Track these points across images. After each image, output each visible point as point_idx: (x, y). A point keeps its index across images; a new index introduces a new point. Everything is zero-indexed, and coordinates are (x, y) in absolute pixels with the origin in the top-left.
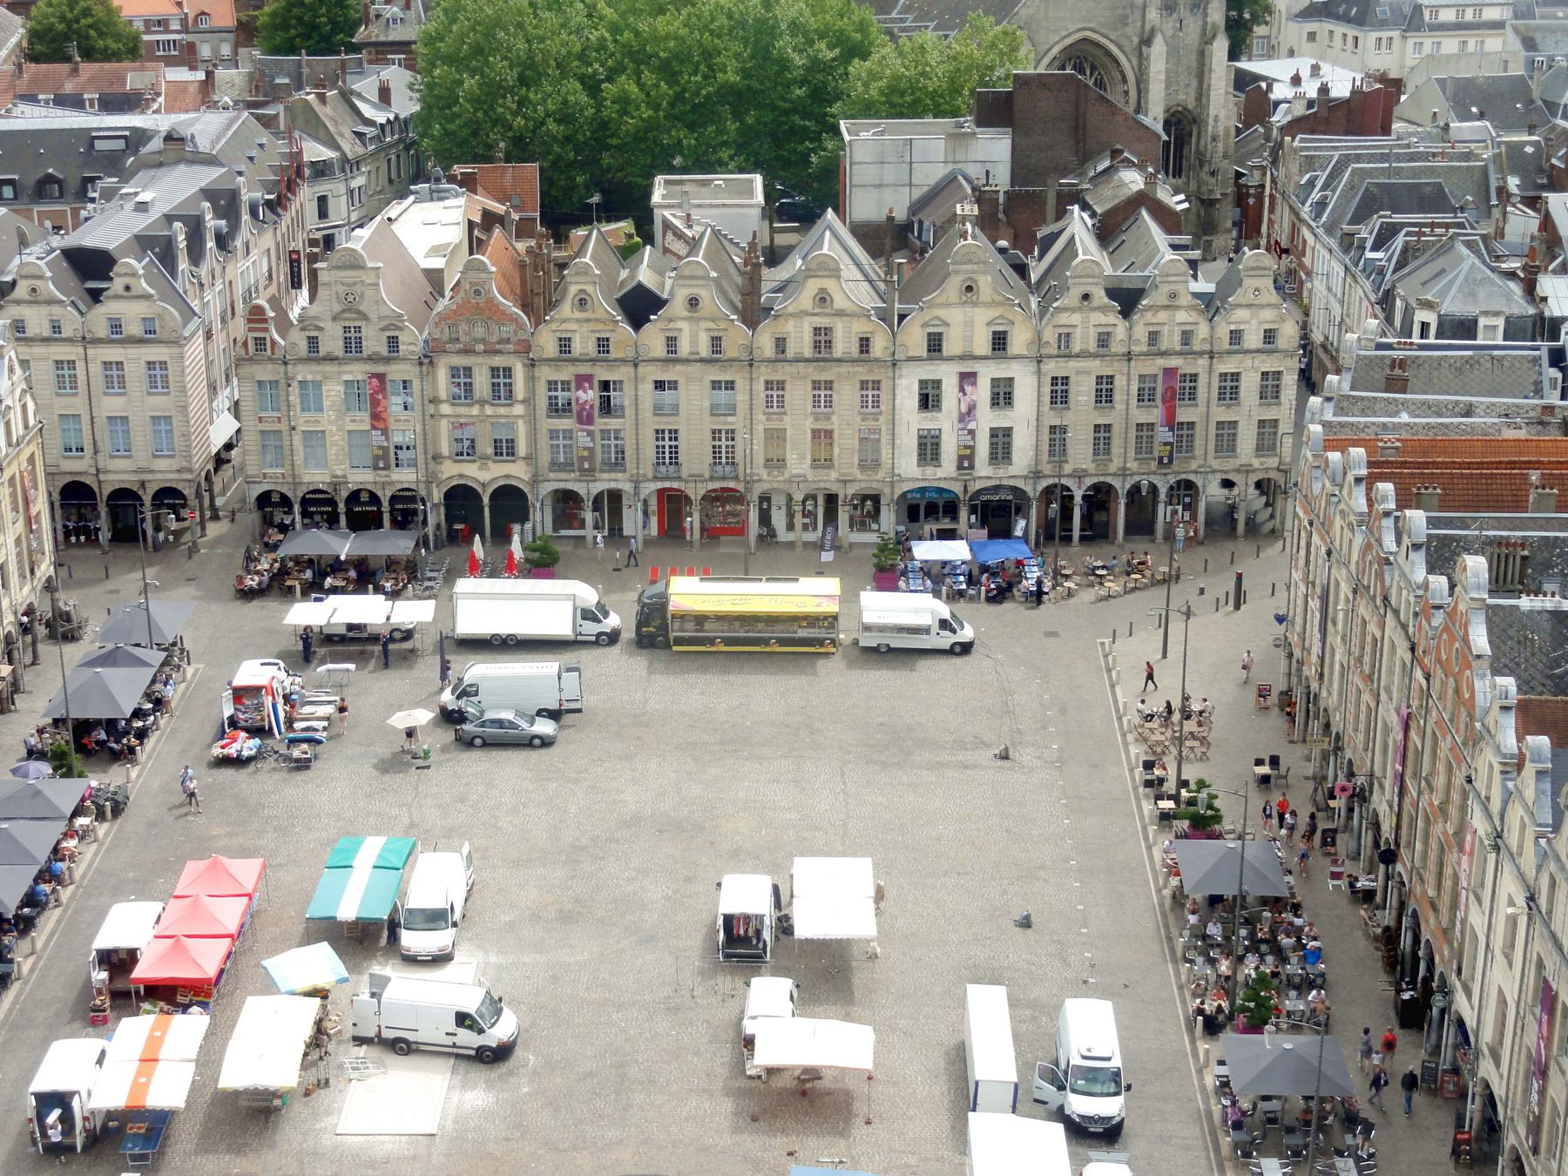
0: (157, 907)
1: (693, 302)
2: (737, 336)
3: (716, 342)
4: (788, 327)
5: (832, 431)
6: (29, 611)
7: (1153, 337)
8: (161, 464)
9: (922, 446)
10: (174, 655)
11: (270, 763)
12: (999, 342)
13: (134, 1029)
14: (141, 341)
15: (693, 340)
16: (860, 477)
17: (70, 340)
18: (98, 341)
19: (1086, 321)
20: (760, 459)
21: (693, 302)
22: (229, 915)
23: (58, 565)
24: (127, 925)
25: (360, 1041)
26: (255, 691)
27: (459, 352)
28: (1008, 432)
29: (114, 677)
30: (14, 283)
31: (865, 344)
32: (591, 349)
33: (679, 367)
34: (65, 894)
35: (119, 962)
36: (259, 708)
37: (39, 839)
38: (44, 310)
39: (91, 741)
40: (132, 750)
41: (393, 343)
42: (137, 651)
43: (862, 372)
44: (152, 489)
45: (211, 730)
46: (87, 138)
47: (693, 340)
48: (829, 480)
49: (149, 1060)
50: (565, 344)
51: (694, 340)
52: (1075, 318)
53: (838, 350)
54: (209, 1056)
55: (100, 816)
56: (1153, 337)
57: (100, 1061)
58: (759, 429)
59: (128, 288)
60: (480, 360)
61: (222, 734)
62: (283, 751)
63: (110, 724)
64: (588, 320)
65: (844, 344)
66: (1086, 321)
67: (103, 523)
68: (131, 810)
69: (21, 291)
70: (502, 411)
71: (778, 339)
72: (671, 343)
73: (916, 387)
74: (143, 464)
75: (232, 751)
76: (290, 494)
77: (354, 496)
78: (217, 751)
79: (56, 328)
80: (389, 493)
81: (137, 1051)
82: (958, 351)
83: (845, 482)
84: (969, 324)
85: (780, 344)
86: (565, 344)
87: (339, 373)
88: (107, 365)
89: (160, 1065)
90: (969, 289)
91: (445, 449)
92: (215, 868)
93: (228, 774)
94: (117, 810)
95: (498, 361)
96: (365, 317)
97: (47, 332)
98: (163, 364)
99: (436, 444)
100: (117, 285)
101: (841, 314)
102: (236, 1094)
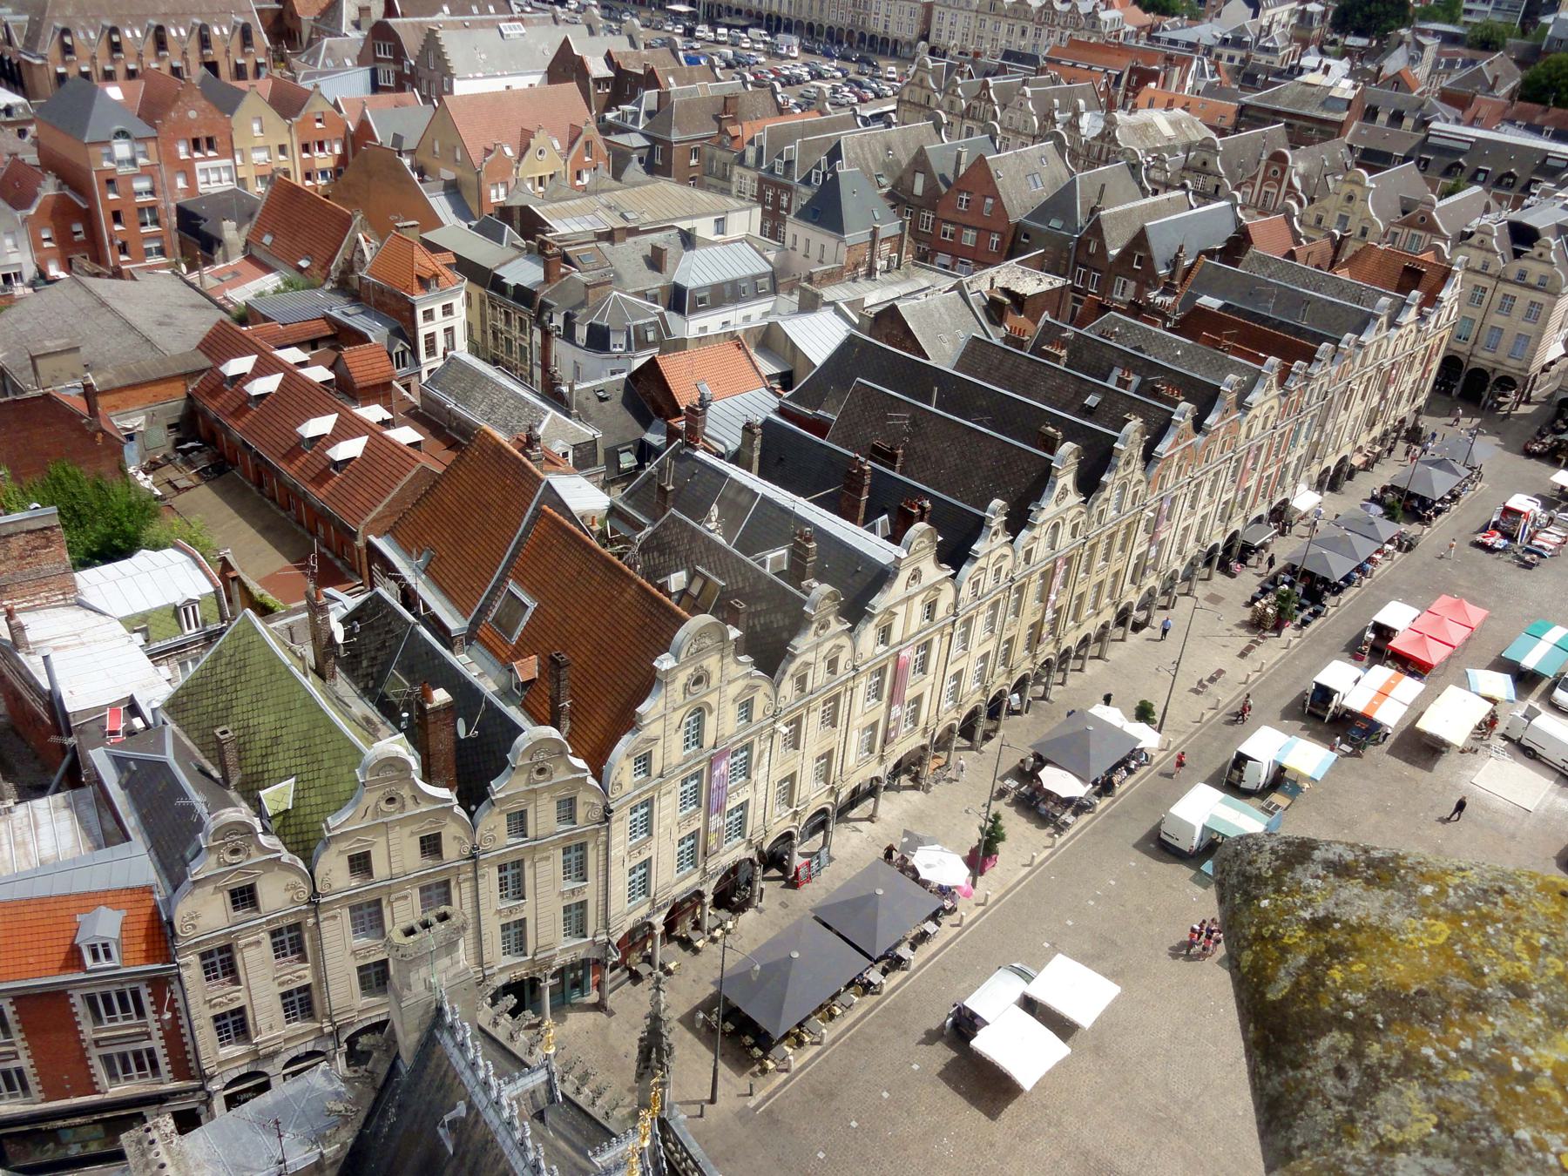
0: (1416, 612)
6: (1403, 421)
8: (1511, 362)
10: (1475, 473)
11: (1509, 557)
13: (1382, 673)
14: (1533, 288)
17: (1490, 276)
22: (1457, 634)
23: (1429, 401)
24: (1397, 615)
25: (1505, 737)
26: (1519, 513)
29: (1436, 473)
30: (1472, 234)
34: (1366, 581)
35: (1384, 632)
36: (1517, 523)
37: (1365, 548)
38: (1484, 254)
39: (1408, 505)
40: (1430, 518)
42: (1455, 465)
44: (1499, 374)
45: (1478, 526)
46: (1545, 155)
49: (1383, 694)
54: (1417, 709)
55: (1399, 548)
57: (1357, 682)
61: (1485, 529)
62: (1520, 553)
63: (1422, 500)
67: (1460, 384)
68: (1416, 552)
69: (1474, 240)
75: (1490, 541)
78: (1479, 538)
79: (1485, 266)
81: (1378, 685)
88: (1506, 296)
89: (1378, 687)
92: (1458, 605)
93: (1481, 553)
94: (1409, 549)
97: (1478, 268)
98: (1541, 305)
100: (1534, 252)
102: (1423, 734)
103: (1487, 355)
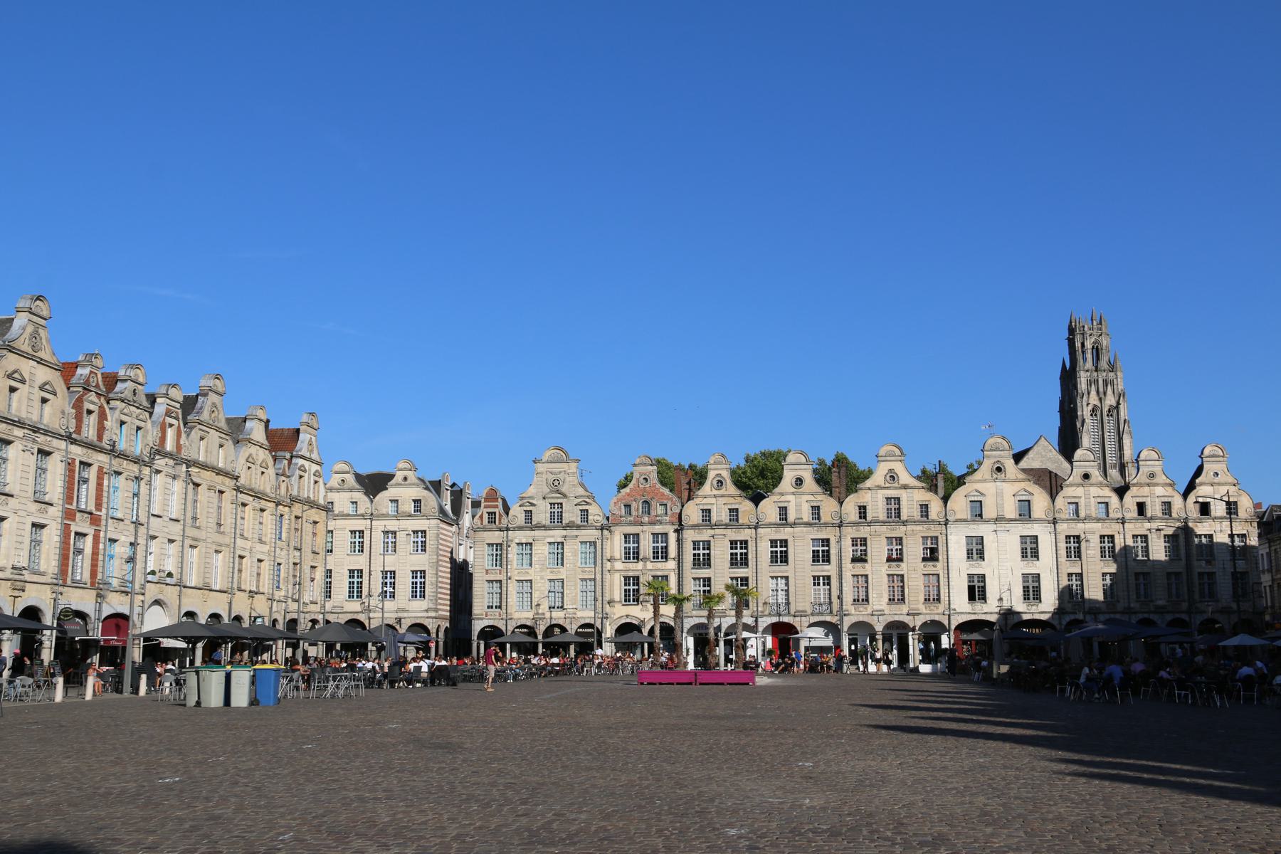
1: (799, 481)
2: (829, 506)
3: (816, 510)
4: (864, 497)
5: (902, 576)
7: (1141, 507)
9: (971, 590)
12: (1025, 511)
15: (799, 506)
16: (924, 611)
17: (363, 516)
18: (385, 516)
19: (1087, 494)
20: (848, 597)
21: (799, 481)
27: (630, 524)
28: (1037, 577)
31: (925, 508)
32: (725, 517)
33: (788, 530)
41: (585, 513)
43: (921, 530)
44: (406, 624)
47: (799, 506)
48: (899, 613)
50: (707, 513)
51: (798, 510)
52: (1079, 491)
53: (904, 516)
56: (1141, 507)
58: (847, 576)
59: (405, 479)
60: (645, 528)
64: (723, 496)
65: (909, 509)
66: (1087, 494)
70: (659, 565)
71: (860, 507)
72: (783, 511)
73: (964, 541)
74: (401, 606)
76: (503, 629)
77: (549, 630)
80: (575, 627)
82: (994, 515)
83: (914, 615)
84: (999, 494)
85: (863, 510)
86: (707, 513)
87: (545, 537)
88: (386, 533)
90: (999, 469)
91: (618, 594)
95: (658, 529)
96: (565, 496)
97: (349, 509)
99: (611, 591)
101: (905, 487)
103: (389, 605)
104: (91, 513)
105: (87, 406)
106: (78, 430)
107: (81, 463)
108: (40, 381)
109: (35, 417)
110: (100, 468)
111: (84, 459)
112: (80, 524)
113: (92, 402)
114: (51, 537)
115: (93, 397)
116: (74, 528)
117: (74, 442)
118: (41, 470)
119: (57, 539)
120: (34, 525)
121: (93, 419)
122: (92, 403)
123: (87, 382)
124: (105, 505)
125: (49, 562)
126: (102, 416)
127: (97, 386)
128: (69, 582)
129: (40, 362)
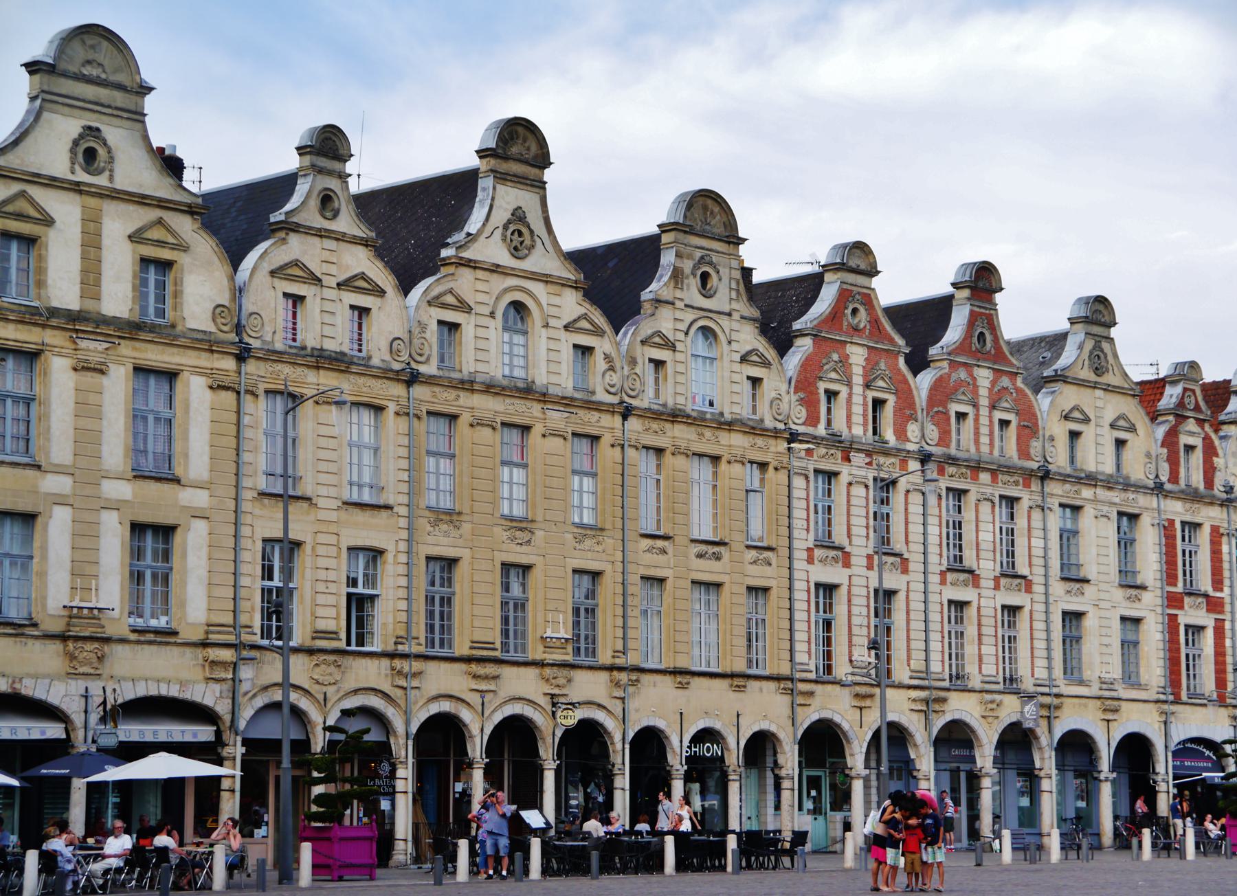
104: (1206, 596)
105: (1184, 439)
106: (1174, 478)
107: (1183, 523)
108: (1109, 416)
109: (1108, 467)
110: (1215, 530)
111: (1188, 518)
112: (1192, 612)
113: (1191, 434)
114: (1152, 636)
115: (1191, 425)
116: (1184, 618)
117: (1167, 495)
118: (1126, 544)
119: (1159, 636)
120: (1124, 619)
121: (1197, 457)
122: (1192, 434)
123: (1181, 404)
124: (1227, 582)
125: (1153, 670)
126: (1210, 451)
127: (1197, 408)
128: (1184, 698)
129: (1109, 389)
